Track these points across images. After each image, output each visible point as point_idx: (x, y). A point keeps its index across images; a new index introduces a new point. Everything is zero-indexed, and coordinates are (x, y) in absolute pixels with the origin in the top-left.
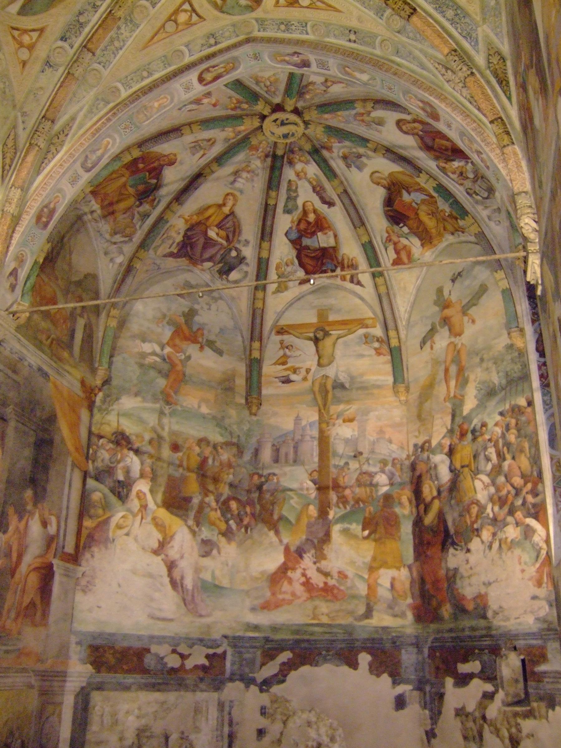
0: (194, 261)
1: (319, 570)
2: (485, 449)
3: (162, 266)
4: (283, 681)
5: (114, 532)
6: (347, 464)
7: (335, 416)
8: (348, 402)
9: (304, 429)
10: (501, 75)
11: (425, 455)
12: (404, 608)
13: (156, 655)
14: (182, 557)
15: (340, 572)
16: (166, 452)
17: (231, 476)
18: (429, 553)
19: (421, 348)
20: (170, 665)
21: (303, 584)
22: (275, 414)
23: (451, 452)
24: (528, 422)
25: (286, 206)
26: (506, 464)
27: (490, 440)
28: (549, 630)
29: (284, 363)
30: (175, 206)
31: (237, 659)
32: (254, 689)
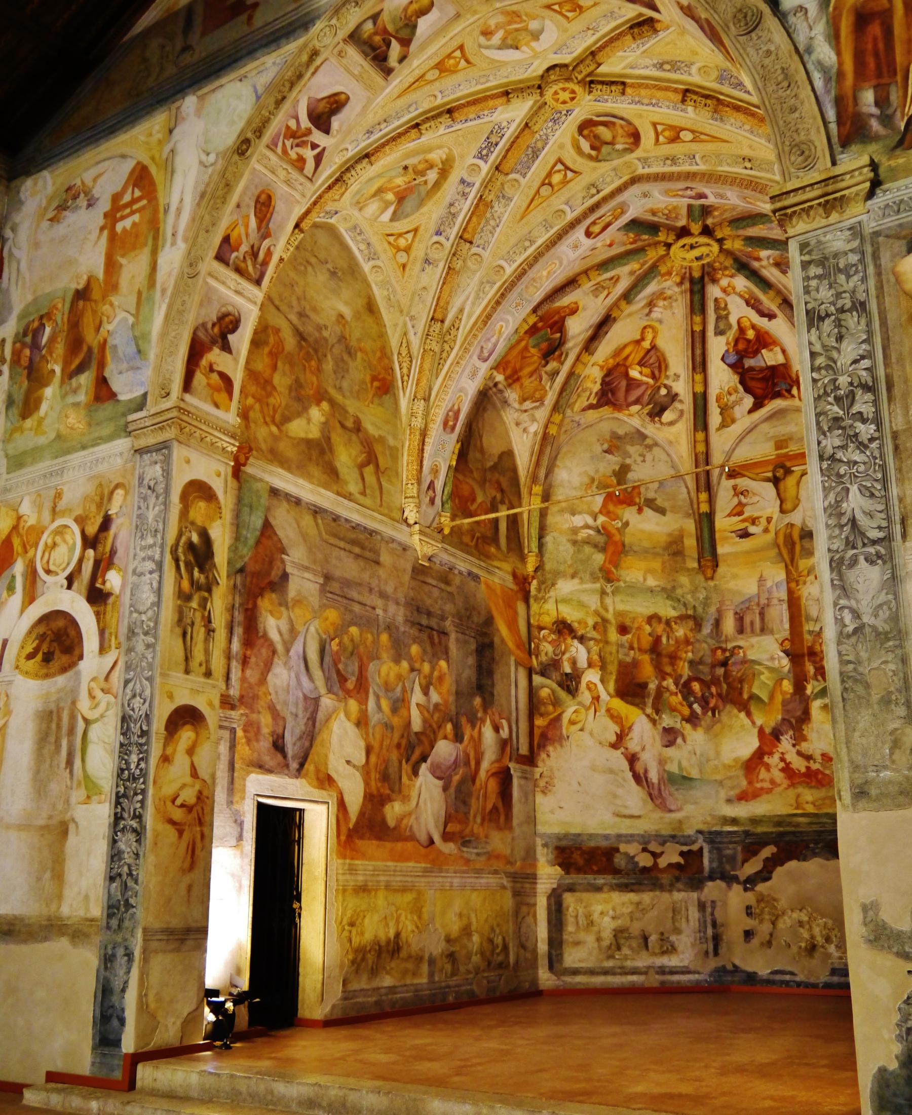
0: (617, 406)
1: (799, 753)
3: (582, 422)
4: (769, 879)
5: (567, 729)
7: (805, 573)
9: (769, 591)
13: (626, 854)
14: (643, 749)
15: (823, 755)
16: (613, 635)
17: (690, 655)
20: (642, 864)
22: (735, 576)
29: (740, 513)
30: (585, 357)
31: (715, 856)
32: (737, 888)
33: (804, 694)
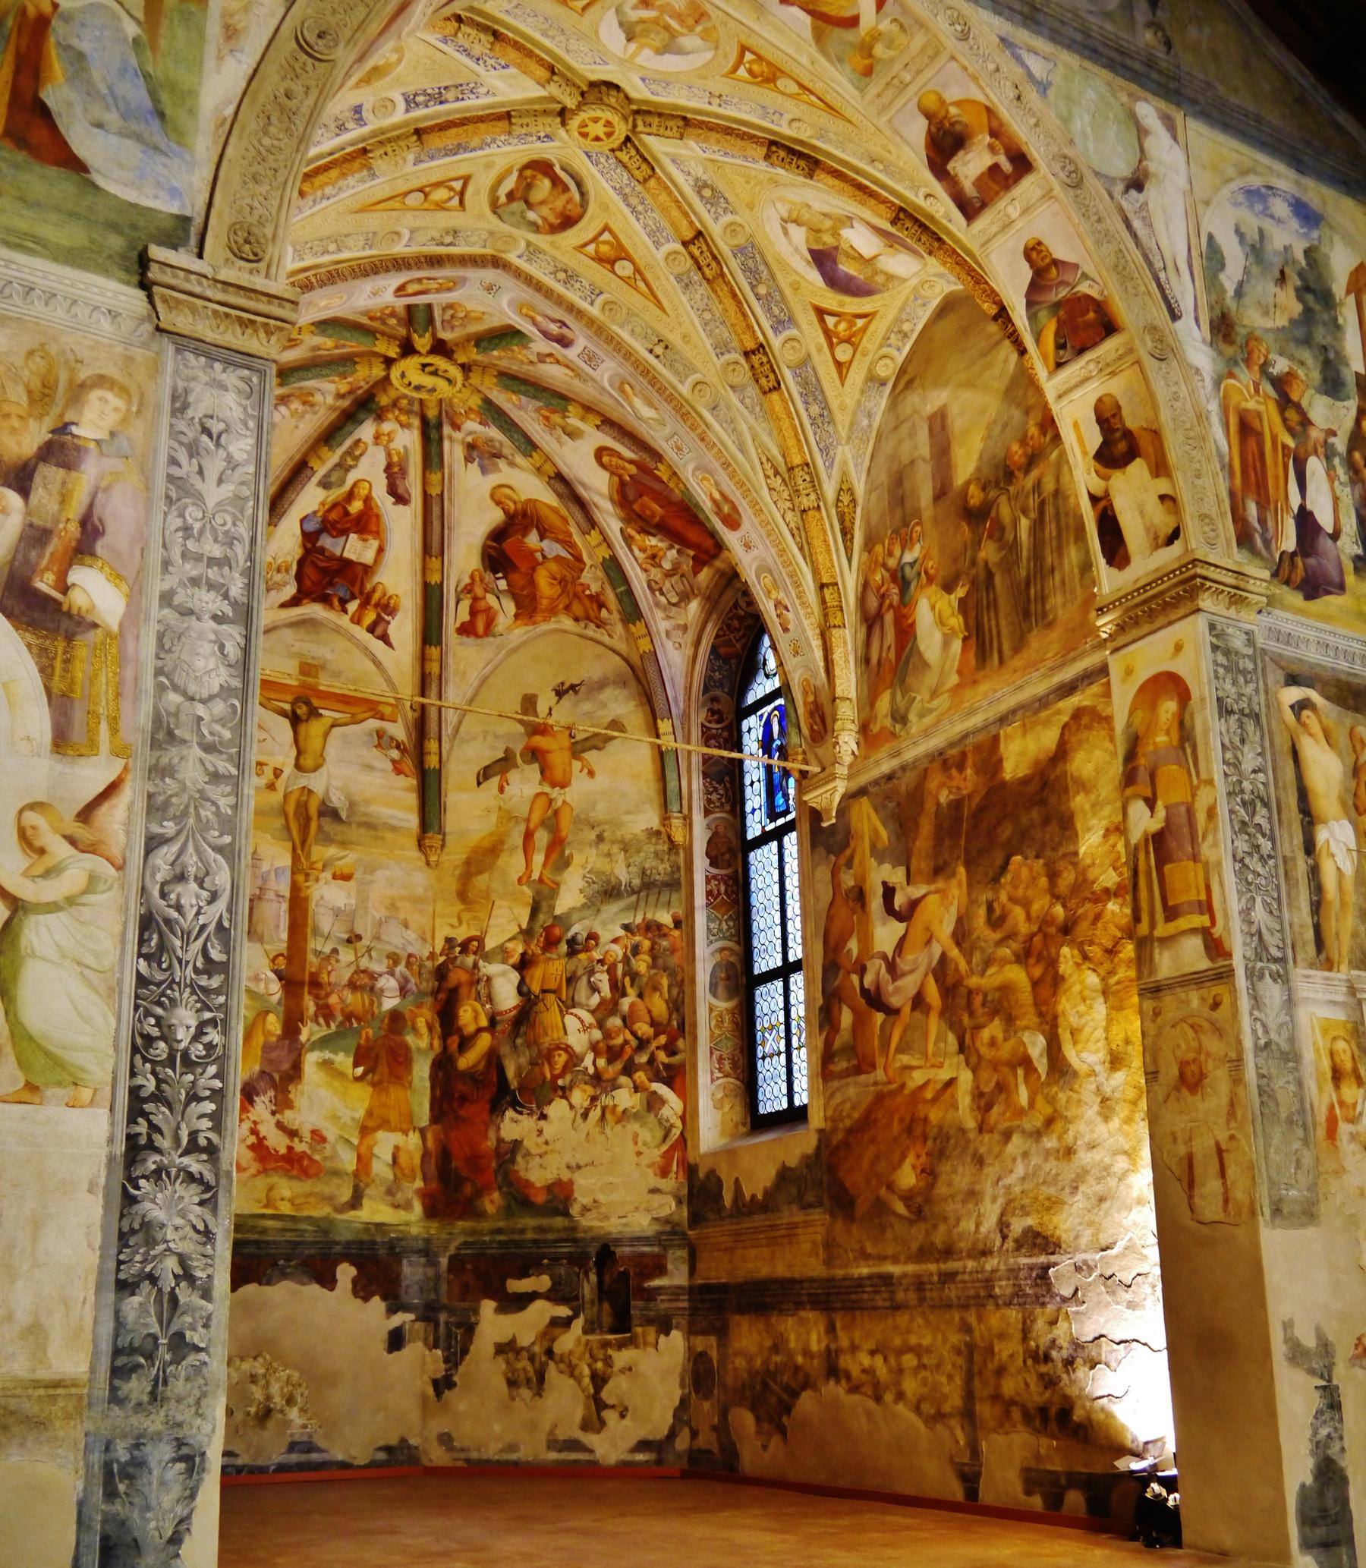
1: (280, 1125)
2: (592, 972)
6: (335, 951)
7: (319, 865)
8: (343, 844)
9: (264, 878)
10: (847, 524)
11: (470, 960)
15: (313, 1132)
18: (463, 1113)
19: (479, 784)
21: (252, 1147)
23: (523, 965)
24: (673, 950)
26: (625, 1003)
27: (601, 962)
28: (673, 1233)
33: (297, 1039)
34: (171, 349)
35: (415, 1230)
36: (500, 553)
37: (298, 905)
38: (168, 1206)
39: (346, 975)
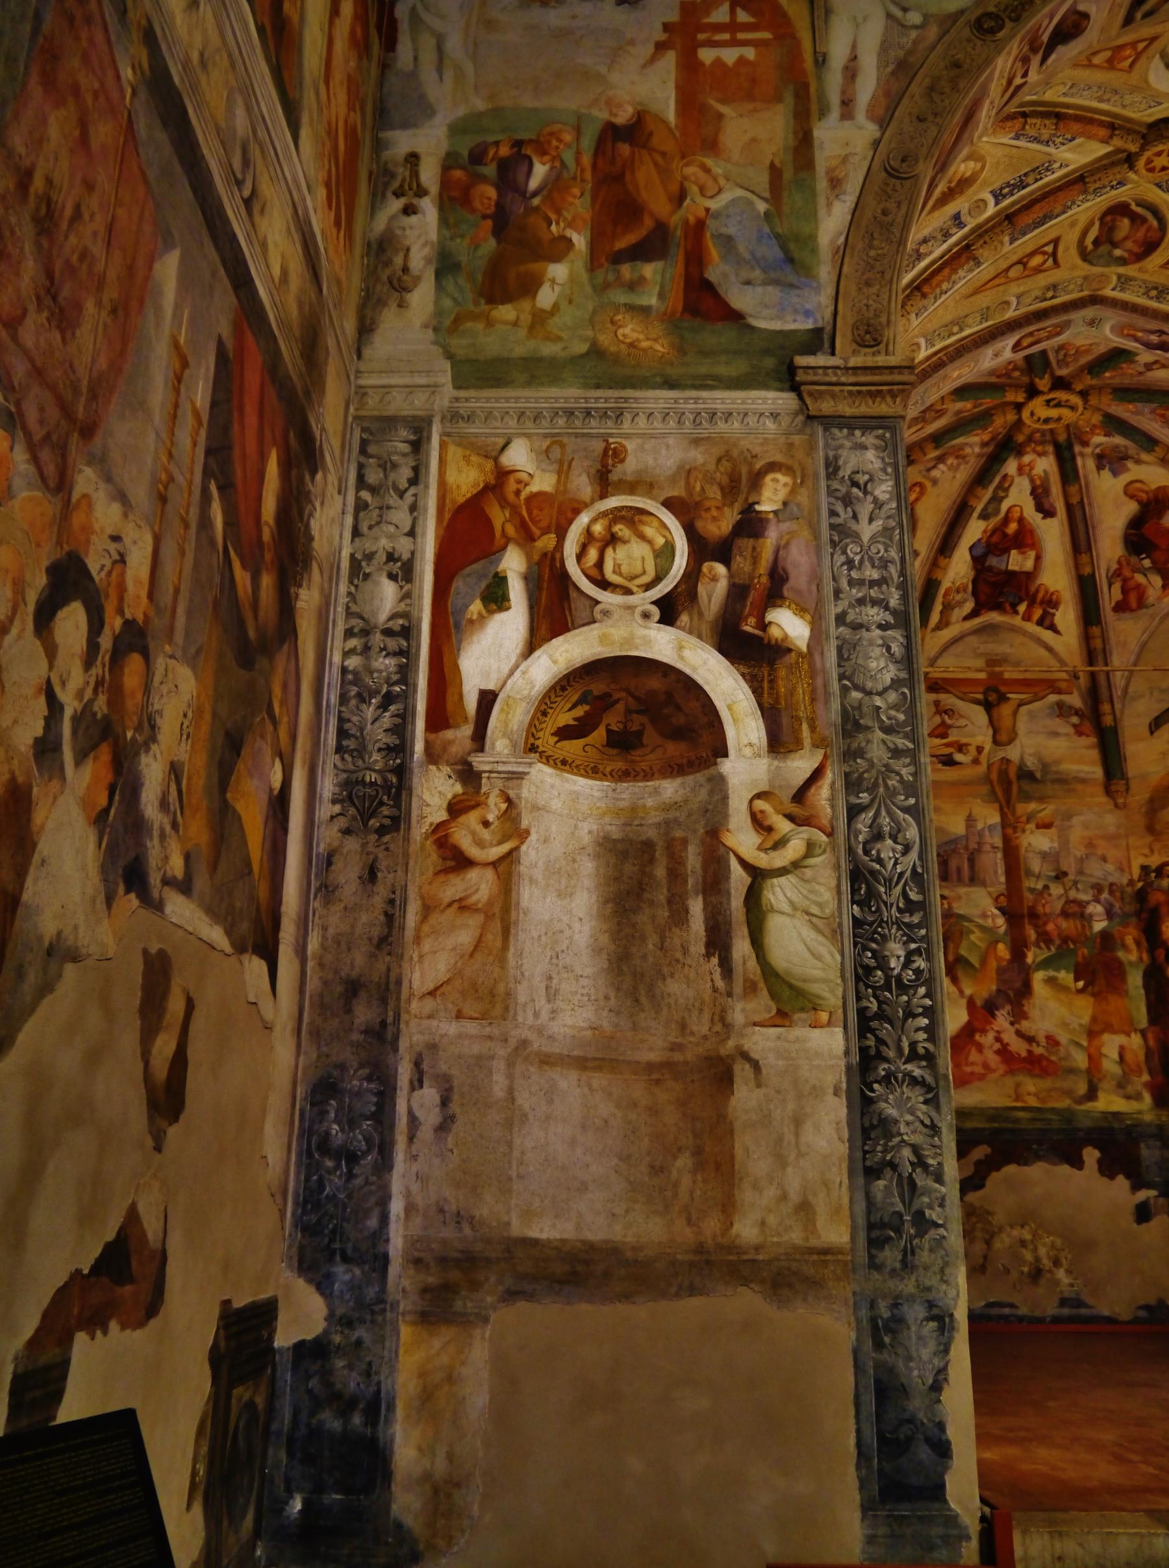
1: (1019, 1033)
6: (1046, 887)
7: (1024, 819)
8: (1041, 799)
9: (980, 834)
12: (1139, 1088)
19: (1152, 733)
21: (998, 1052)
25: (985, 509)
29: (944, 736)
34: (820, 430)
35: (1148, 1117)
36: (1138, 537)
37: (1011, 853)
38: (898, 1105)
39: (1059, 905)
